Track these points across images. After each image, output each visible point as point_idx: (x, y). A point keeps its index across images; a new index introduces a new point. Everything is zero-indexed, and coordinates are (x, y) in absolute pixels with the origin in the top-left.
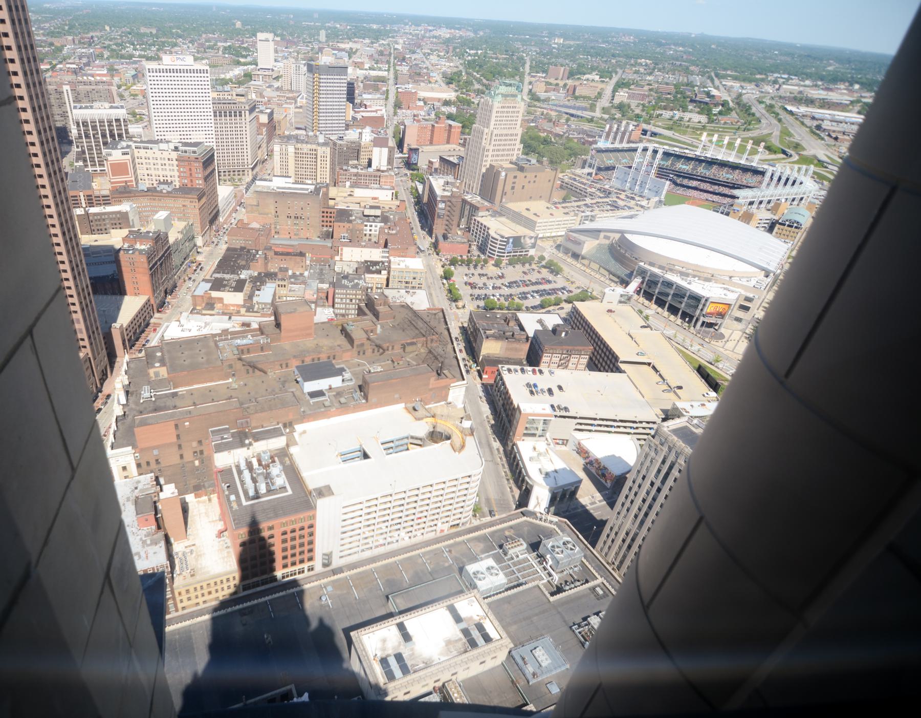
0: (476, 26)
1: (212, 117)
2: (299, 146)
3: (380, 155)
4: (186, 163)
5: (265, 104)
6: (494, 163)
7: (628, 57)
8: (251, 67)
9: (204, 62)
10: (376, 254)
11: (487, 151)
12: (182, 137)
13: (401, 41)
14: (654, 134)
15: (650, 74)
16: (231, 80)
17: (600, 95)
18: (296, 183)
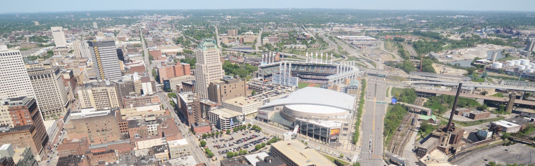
0: (185, 13)
1: (30, 80)
2: (94, 89)
3: (147, 87)
4: (16, 111)
5: (66, 67)
6: (212, 82)
7: (264, 22)
8: (51, 48)
9: (16, 48)
10: (159, 142)
11: (207, 75)
12: (10, 95)
13: (144, 24)
14: (285, 56)
15: (276, 29)
16: (39, 57)
17: (256, 41)
18: (98, 110)
